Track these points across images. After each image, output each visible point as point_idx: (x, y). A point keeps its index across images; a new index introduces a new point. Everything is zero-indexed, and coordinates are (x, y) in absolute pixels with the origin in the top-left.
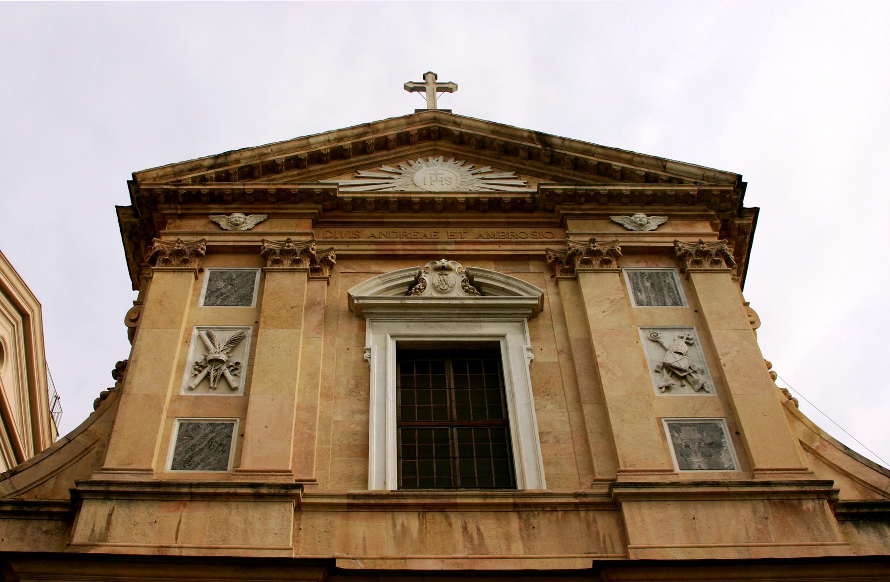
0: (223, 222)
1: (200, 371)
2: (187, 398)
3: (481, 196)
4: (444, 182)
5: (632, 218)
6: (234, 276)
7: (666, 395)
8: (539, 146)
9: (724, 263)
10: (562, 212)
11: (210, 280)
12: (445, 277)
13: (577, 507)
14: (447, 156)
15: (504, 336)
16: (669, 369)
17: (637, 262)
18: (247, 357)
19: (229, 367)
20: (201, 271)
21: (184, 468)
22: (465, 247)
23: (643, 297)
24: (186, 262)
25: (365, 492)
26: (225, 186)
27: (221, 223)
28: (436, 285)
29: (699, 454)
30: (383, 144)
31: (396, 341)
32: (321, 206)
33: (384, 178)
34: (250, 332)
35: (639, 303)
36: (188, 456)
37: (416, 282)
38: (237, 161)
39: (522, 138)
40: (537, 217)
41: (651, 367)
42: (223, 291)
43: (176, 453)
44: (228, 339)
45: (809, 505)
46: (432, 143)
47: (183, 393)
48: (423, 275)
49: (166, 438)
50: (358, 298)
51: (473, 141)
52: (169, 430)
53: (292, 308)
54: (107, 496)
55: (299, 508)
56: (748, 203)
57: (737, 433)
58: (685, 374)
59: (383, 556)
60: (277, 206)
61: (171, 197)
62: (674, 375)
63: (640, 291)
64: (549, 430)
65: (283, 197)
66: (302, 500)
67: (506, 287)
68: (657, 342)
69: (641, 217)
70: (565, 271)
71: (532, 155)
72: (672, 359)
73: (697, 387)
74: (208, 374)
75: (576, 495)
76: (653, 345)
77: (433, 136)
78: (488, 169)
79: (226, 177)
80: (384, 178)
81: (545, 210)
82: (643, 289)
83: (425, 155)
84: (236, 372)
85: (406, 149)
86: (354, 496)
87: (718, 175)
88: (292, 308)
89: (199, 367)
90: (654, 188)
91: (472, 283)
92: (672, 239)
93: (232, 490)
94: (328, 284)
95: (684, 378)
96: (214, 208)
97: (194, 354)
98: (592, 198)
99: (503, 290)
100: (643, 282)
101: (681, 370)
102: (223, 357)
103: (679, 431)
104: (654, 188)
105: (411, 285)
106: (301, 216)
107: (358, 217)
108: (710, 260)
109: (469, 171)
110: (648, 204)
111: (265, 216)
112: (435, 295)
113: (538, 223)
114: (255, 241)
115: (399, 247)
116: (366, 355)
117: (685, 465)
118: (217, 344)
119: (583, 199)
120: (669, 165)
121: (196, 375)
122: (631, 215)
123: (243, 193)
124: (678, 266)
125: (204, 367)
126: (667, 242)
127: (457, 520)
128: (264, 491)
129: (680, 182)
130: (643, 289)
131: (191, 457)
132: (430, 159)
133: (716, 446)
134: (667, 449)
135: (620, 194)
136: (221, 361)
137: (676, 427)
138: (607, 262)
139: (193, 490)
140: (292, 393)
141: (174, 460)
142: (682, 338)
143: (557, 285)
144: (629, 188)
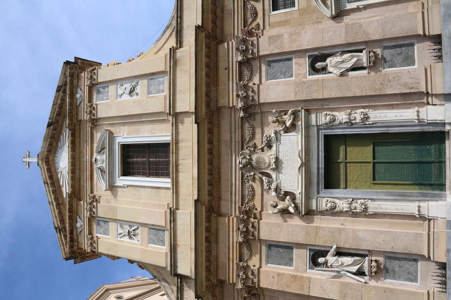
0: (80, 230)
1: (132, 238)
2: (141, 241)
4: (64, 158)
5: (78, 99)
8: (52, 127)
9: (94, 71)
10: (75, 121)
11: (100, 234)
12: (98, 160)
15: (119, 143)
16: (131, 92)
17: (93, 98)
19: (130, 229)
20: (97, 237)
22: (88, 153)
23: (105, 98)
24: (94, 242)
25: (171, 189)
26: (68, 229)
29: (159, 86)
30: (51, 177)
31: (121, 176)
32: (74, 199)
33: (63, 177)
35: (108, 99)
36: (161, 242)
37: (100, 169)
38: (58, 225)
39: (49, 132)
40: (77, 129)
42: (104, 230)
43: (160, 245)
44: (121, 229)
46: (50, 161)
47: (139, 243)
48: (98, 167)
49: (155, 248)
50: (106, 187)
51: (49, 148)
52: (152, 247)
53: (110, 208)
55: (177, 209)
56: (73, 61)
57: (152, 74)
59: (192, 184)
60: (74, 212)
61: (71, 247)
62: (133, 91)
64: (150, 131)
65: (71, 211)
66: (175, 208)
67: (102, 141)
68: (121, 95)
69: (78, 96)
70: (97, 121)
71: (55, 129)
72: (128, 91)
74: (133, 235)
75: (173, 126)
76: (122, 96)
77: (48, 161)
78: (59, 143)
79: (65, 228)
80: (63, 177)
81: (75, 126)
82: (103, 98)
83: (54, 164)
84: (132, 226)
85: (52, 170)
86: (173, 192)
87: (63, 70)
88: (110, 208)
89: (130, 237)
90: (68, 91)
91: (101, 151)
92: (86, 87)
93: (172, 229)
94: (101, 197)
95: (133, 88)
96: (75, 232)
97: (126, 239)
98: (71, 112)
99: (103, 142)
100: (100, 97)
101: (131, 89)
103: (152, 92)
104: (68, 91)
105: (101, 171)
106: (77, 205)
107: (77, 186)
108: (93, 75)
110: (73, 93)
111: (78, 216)
112: (105, 163)
113: (79, 129)
114: (86, 220)
116: (125, 186)
117: (163, 91)
118: (122, 232)
119: (71, 114)
120: (60, 85)
121: (133, 239)
122: (77, 99)
123: (70, 223)
124: (95, 85)
125: (131, 236)
126: (87, 89)
127: (180, 162)
128: (172, 219)
129: (66, 82)
130: (103, 98)
131: (161, 241)
132: (56, 162)
134: (157, 96)
135: (70, 102)
138: (94, 109)
140: (139, 210)
141: (162, 246)
142: (120, 87)
144: (68, 99)
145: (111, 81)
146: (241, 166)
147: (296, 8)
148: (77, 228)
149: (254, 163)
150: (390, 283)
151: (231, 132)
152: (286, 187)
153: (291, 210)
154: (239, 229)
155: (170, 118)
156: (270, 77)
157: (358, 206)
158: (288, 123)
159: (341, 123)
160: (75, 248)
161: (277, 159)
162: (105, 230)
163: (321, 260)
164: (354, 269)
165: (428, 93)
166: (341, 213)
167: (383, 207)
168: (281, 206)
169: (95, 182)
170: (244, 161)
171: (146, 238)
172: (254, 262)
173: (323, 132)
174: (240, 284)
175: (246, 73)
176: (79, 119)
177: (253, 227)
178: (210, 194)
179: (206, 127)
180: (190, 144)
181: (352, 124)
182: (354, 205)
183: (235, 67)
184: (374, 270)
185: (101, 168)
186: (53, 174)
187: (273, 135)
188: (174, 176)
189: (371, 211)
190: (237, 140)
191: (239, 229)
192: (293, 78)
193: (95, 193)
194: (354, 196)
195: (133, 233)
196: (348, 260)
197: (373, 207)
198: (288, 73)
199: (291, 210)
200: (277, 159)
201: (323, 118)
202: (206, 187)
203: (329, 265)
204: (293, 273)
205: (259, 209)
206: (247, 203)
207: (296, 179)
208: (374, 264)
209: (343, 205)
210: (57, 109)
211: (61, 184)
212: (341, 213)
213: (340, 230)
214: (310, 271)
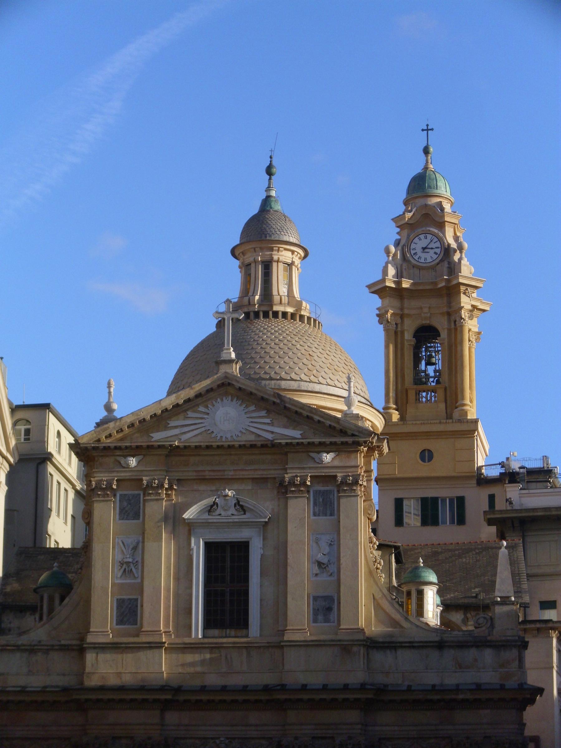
0: (122, 461)
3: (246, 443)
5: (319, 456)
6: (131, 498)
10: (286, 450)
11: (120, 501)
13: (268, 647)
14: (232, 396)
15: (251, 538)
18: (140, 557)
19: (133, 564)
21: (121, 625)
23: (317, 510)
27: (121, 462)
28: (223, 506)
34: (141, 539)
42: (126, 509)
43: (117, 617)
44: (131, 547)
45: (355, 649)
54: (95, 648)
58: (325, 566)
61: (94, 448)
63: (316, 506)
70: (283, 493)
71: (274, 403)
73: (329, 574)
75: (268, 643)
78: (252, 408)
84: (136, 567)
85: (211, 394)
95: (325, 568)
96: (118, 453)
100: (319, 499)
101: (324, 564)
102: (130, 560)
103: (316, 601)
105: (212, 506)
106: (160, 455)
109: (244, 410)
111: (140, 457)
120: (341, 422)
122: (319, 452)
128: (153, 645)
130: (318, 504)
132: (224, 398)
133: (329, 609)
136: (130, 562)
139: (127, 645)
141: (117, 620)
143: (279, 498)
146: (218, 741)
151: (257, 726)
154: (149, 738)
160: (95, 453)
176: (290, 456)
178: (185, 701)
179: (263, 698)
185: (215, 506)
186: (204, 397)
188: (207, 646)
202: (194, 698)
210: (305, 413)
211: (190, 414)
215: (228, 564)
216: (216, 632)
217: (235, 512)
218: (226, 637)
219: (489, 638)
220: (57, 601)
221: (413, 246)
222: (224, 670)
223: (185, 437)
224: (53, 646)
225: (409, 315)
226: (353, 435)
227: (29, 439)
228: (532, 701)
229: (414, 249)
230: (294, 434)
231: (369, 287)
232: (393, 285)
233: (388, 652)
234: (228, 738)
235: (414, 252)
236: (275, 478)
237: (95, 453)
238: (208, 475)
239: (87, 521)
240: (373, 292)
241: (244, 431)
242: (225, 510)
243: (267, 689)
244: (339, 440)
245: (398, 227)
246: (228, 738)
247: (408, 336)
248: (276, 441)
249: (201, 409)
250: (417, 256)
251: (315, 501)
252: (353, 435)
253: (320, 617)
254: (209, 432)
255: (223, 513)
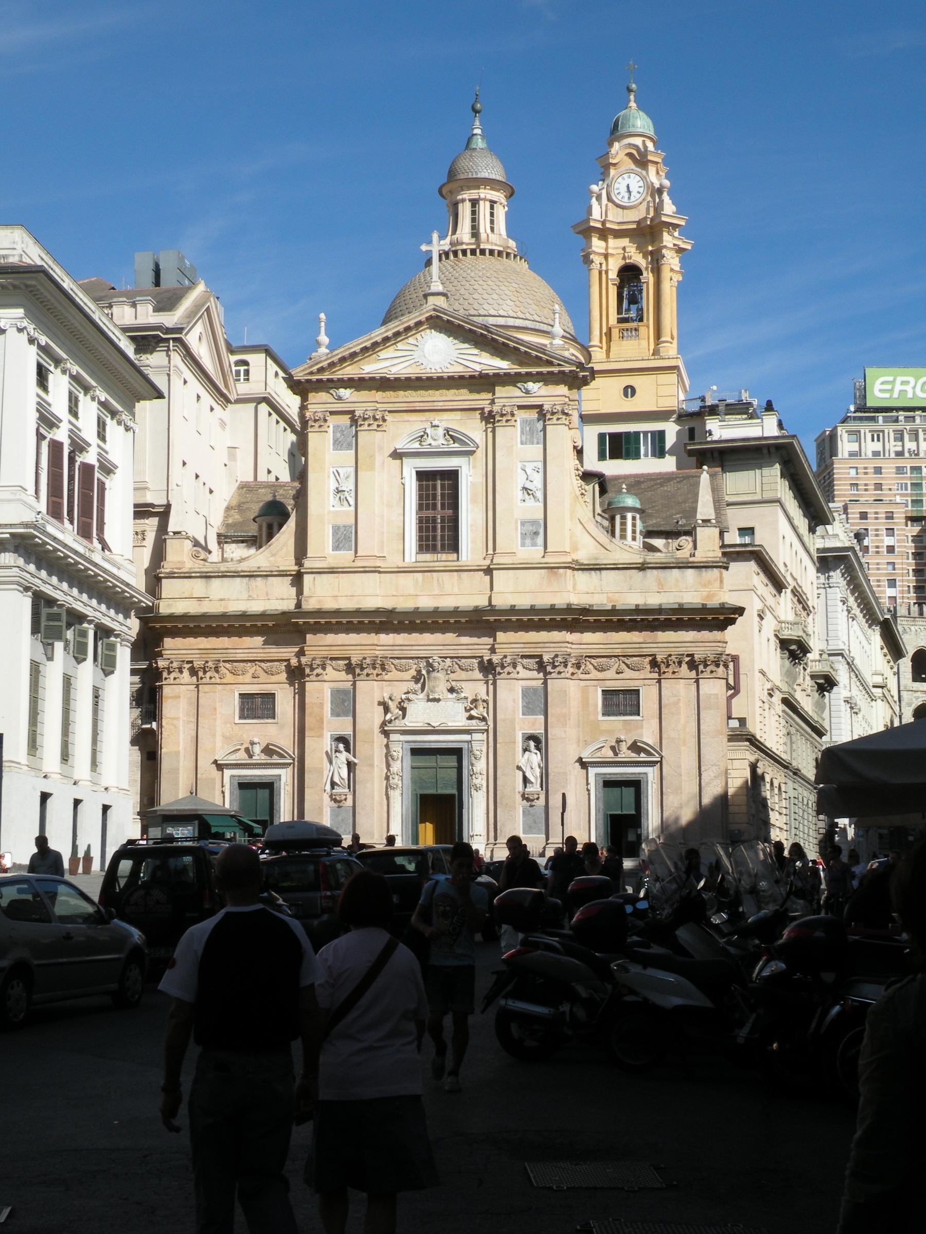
5: (525, 385)
7: (524, 504)
22: (447, 403)
23: (524, 439)
35: (522, 443)
41: (520, 487)
43: (333, 543)
45: (561, 571)
47: (332, 509)
62: (529, 494)
72: (528, 485)
75: (478, 566)
91: (449, 435)
96: (330, 385)
97: (333, 485)
105: (422, 436)
115: (417, 404)
116: (403, 481)
117: (523, 545)
127: (434, 574)
128: (367, 569)
137: (523, 524)
145: (545, 449)
146: (431, 661)
147: (600, 717)
148: (337, 389)
149: (435, 674)
150: (327, 812)
152: (411, 708)
153: (388, 717)
154: (365, 658)
155: (488, 562)
156: (526, 692)
157: (396, 781)
158: (473, 713)
159: (472, 765)
160: (308, 386)
161: (438, 700)
162: (340, 442)
163: (341, 746)
164: (336, 780)
165: (495, 844)
166: (388, 766)
167: (396, 805)
168: (392, 706)
169: (406, 416)
170: (436, 664)
171: (341, 521)
172: (330, 673)
173: (465, 746)
174: (305, 660)
175: (532, 663)
177: (368, 675)
180: (456, 591)
181: (471, 776)
182: (397, 777)
183: (537, 651)
184: (338, 798)
187: (463, 695)
189: (391, 793)
190: (460, 651)
191: (365, 658)
192: (521, 716)
193: (389, 417)
194: (404, 777)
195: (342, 497)
196: (344, 772)
197: (396, 796)
198: (528, 710)
199: (388, 717)
200: (438, 700)
201: (478, 748)
203: (338, 754)
204: (325, 720)
205: (386, 677)
206: (392, 664)
207: (418, 720)
208: (343, 797)
209: (396, 767)
211: (400, 346)
212: (388, 766)
213: (372, 765)
214: (329, 736)
215: (439, 491)
216: (428, 557)
217: (445, 443)
218: (437, 561)
219: (691, 559)
220: (275, 527)
221: (617, 186)
222: (436, 593)
223: (394, 370)
224: (272, 571)
225: (612, 255)
226: (559, 365)
227: (248, 380)
228: (732, 622)
229: (618, 189)
230: (503, 365)
231: (574, 227)
232: (599, 225)
233: (593, 572)
234: (441, 657)
235: (618, 191)
236: (483, 409)
237: (308, 386)
238: (418, 406)
239: (302, 452)
240: (577, 233)
241: (452, 363)
242: (435, 440)
243: (477, 611)
244: (544, 370)
245: (602, 167)
246: (441, 657)
247: (613, 275)
248: (483, 372)
249: (411, 340)
250: (621, 196)
251: (522, 429)
252: (559, 365)
253: (528, 541)
254: (418, 364)
255: (433, 443)
